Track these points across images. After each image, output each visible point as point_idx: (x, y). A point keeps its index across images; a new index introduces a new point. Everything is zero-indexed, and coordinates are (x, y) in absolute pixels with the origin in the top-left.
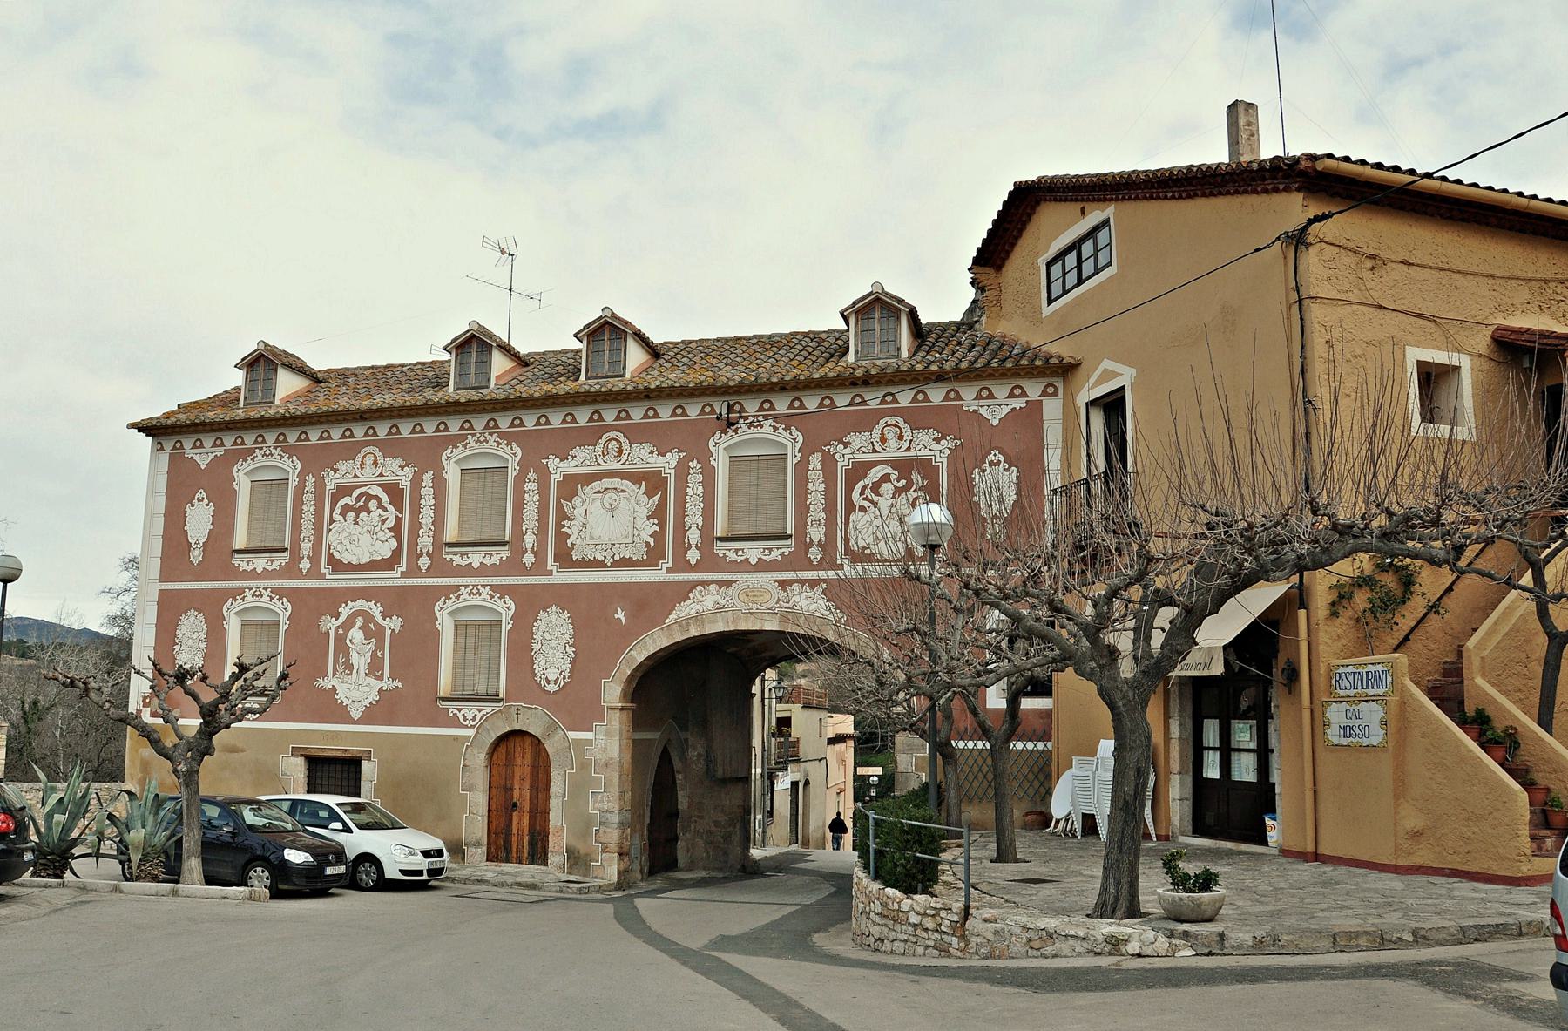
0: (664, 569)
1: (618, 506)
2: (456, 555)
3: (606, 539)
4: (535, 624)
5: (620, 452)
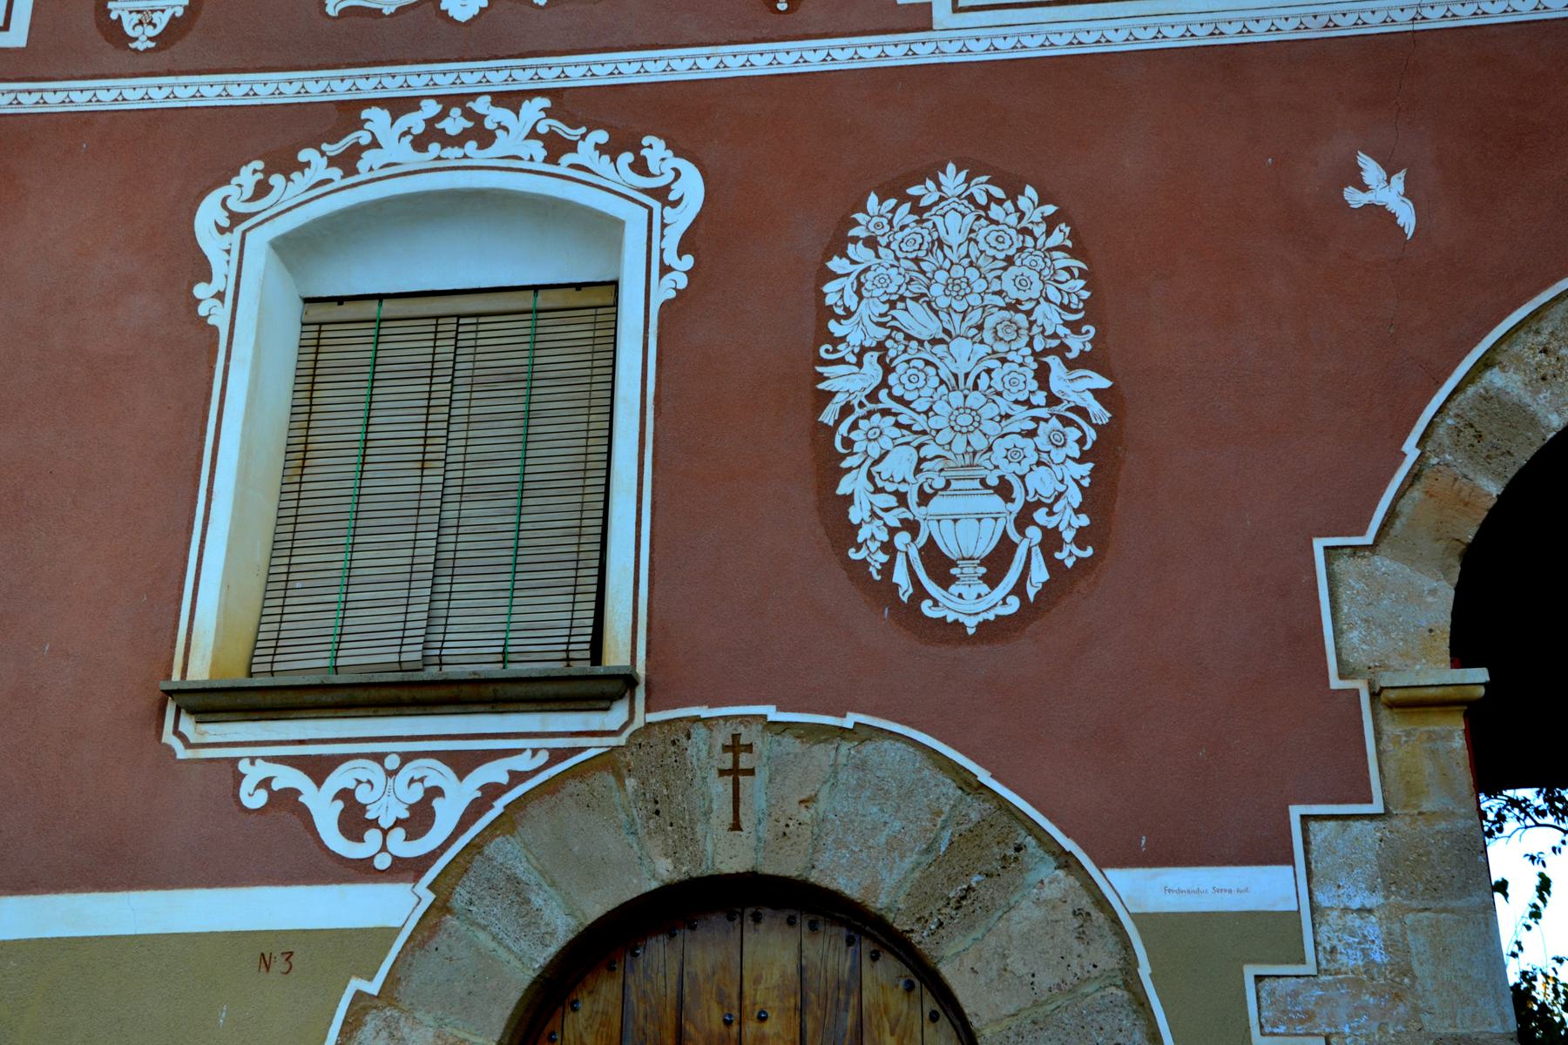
4: (836, 264)
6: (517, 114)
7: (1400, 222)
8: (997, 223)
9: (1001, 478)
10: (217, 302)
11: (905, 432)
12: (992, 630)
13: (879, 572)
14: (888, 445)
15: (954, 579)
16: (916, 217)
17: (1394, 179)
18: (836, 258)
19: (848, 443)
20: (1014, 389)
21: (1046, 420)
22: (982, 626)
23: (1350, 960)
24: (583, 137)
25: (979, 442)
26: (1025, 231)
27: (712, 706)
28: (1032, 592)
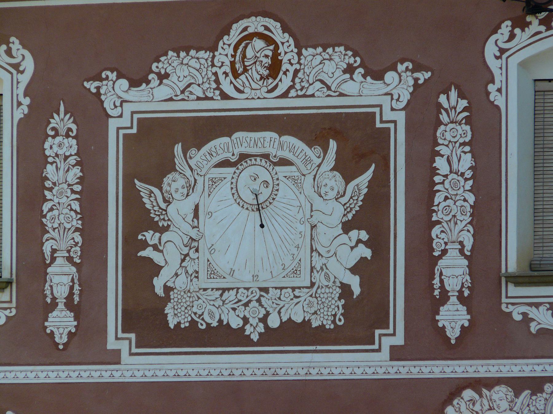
1: (272, 198)
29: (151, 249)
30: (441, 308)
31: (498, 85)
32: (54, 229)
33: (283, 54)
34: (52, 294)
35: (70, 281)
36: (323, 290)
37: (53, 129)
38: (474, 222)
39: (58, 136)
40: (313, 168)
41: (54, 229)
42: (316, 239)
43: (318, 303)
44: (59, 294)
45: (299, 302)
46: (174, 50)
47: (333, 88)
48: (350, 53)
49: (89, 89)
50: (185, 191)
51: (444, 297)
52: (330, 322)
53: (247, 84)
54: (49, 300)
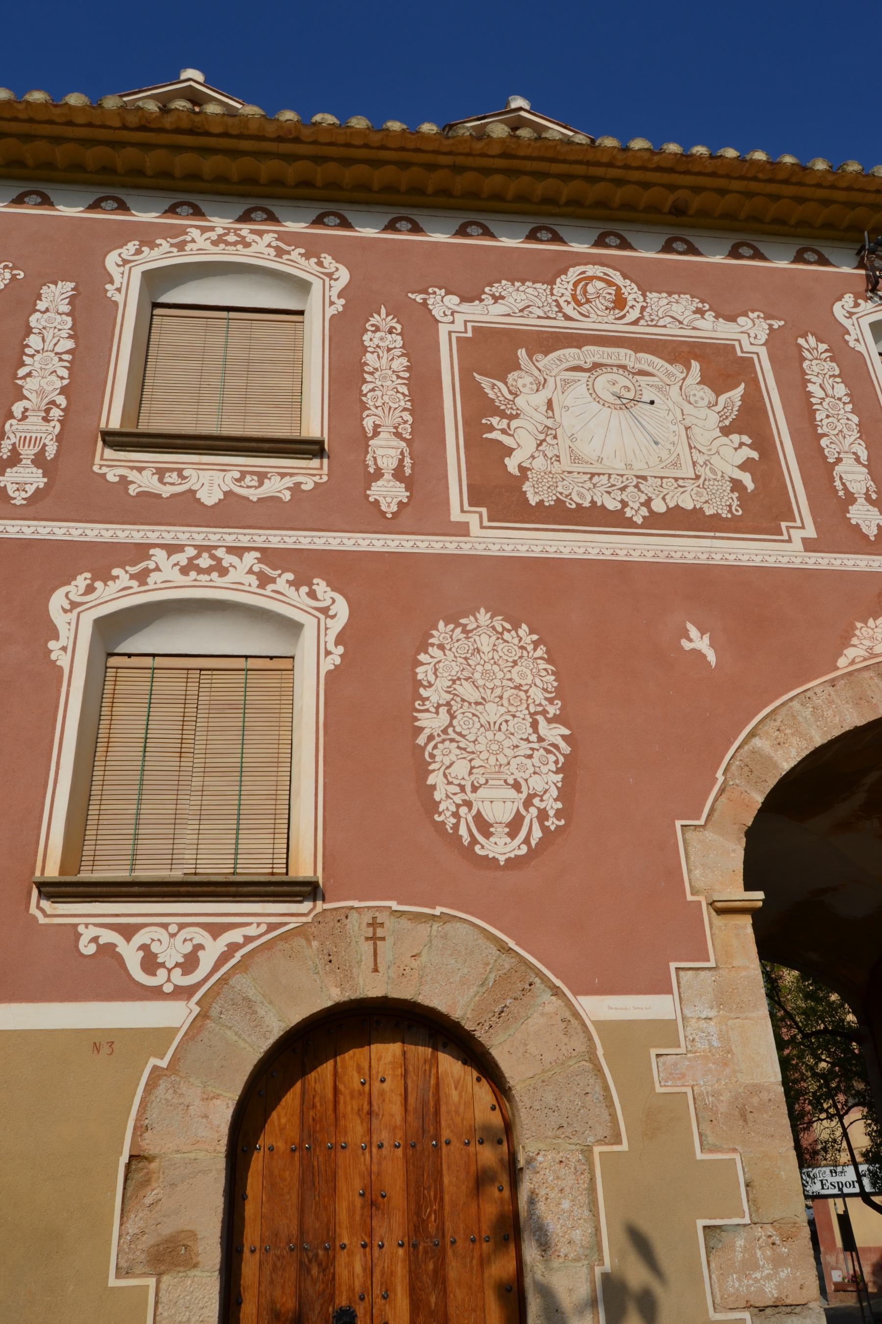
0: (798, 545)
2: (140, 470)
3: (618, 466)
4: (422, 657)
5: (620, 302)
6: (241, 559)
7: (709, 659)
8: (508, 642)
9: (515, 780)
10: (62, 652)
11: (463, 752)
12: (514, 863)
13: (451, 828)
14: (454, 758)
15: (492, 834)
16: (465, 635)
17: (704, 637)
18: (422, 654)
19: (432, 756)
20: (520, 732)
21: (538, 750)
22: (508, 860)
23: (702, 1046)
24: (280, 576)
25: (503, 760)
26: (522, 648)
27: (360, 900)
28: (533, 843)
29: (499, 432)
30: (850, 507)
31: (854, 337)
32: (377, 407)
33: (626, 294)
34: (376, 463)
35: (399, 453)
36: (711, 483)
37: (373, 325)
38: (864, 437)
39: (379, 331)
40: (677, 380)
41: (377, 407)
42: (692, 437)
43: (707, 494)
44: (385, 465)
45: (685, 491)
46: (508, 280)
47: (685, 322)
48: (698, 300)
49: (414, 300)
50: (535, 387)
51: (851, 498)
52: (726, 512)
53: (592, 311)
54: (372, 470)
